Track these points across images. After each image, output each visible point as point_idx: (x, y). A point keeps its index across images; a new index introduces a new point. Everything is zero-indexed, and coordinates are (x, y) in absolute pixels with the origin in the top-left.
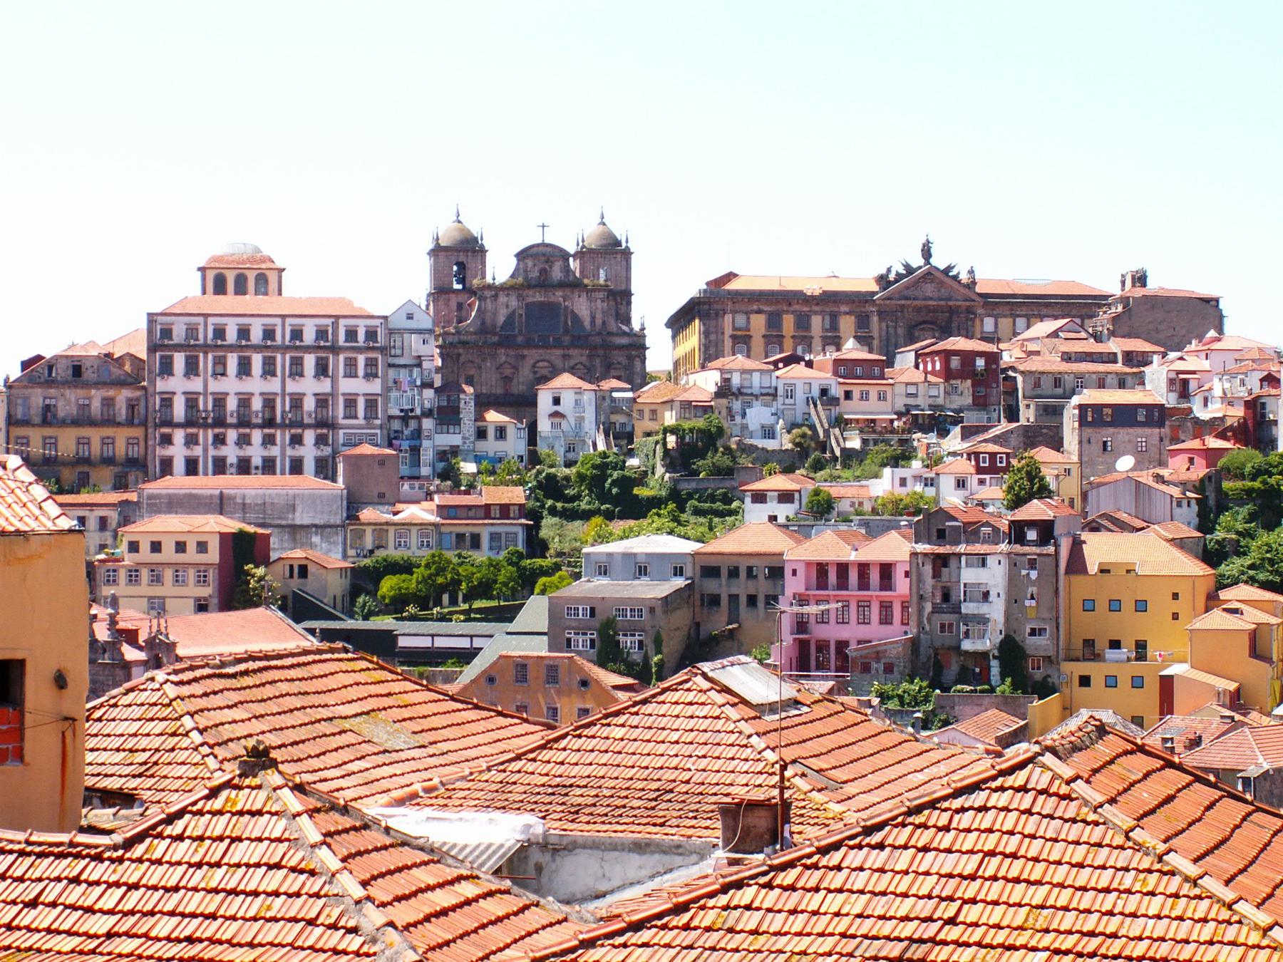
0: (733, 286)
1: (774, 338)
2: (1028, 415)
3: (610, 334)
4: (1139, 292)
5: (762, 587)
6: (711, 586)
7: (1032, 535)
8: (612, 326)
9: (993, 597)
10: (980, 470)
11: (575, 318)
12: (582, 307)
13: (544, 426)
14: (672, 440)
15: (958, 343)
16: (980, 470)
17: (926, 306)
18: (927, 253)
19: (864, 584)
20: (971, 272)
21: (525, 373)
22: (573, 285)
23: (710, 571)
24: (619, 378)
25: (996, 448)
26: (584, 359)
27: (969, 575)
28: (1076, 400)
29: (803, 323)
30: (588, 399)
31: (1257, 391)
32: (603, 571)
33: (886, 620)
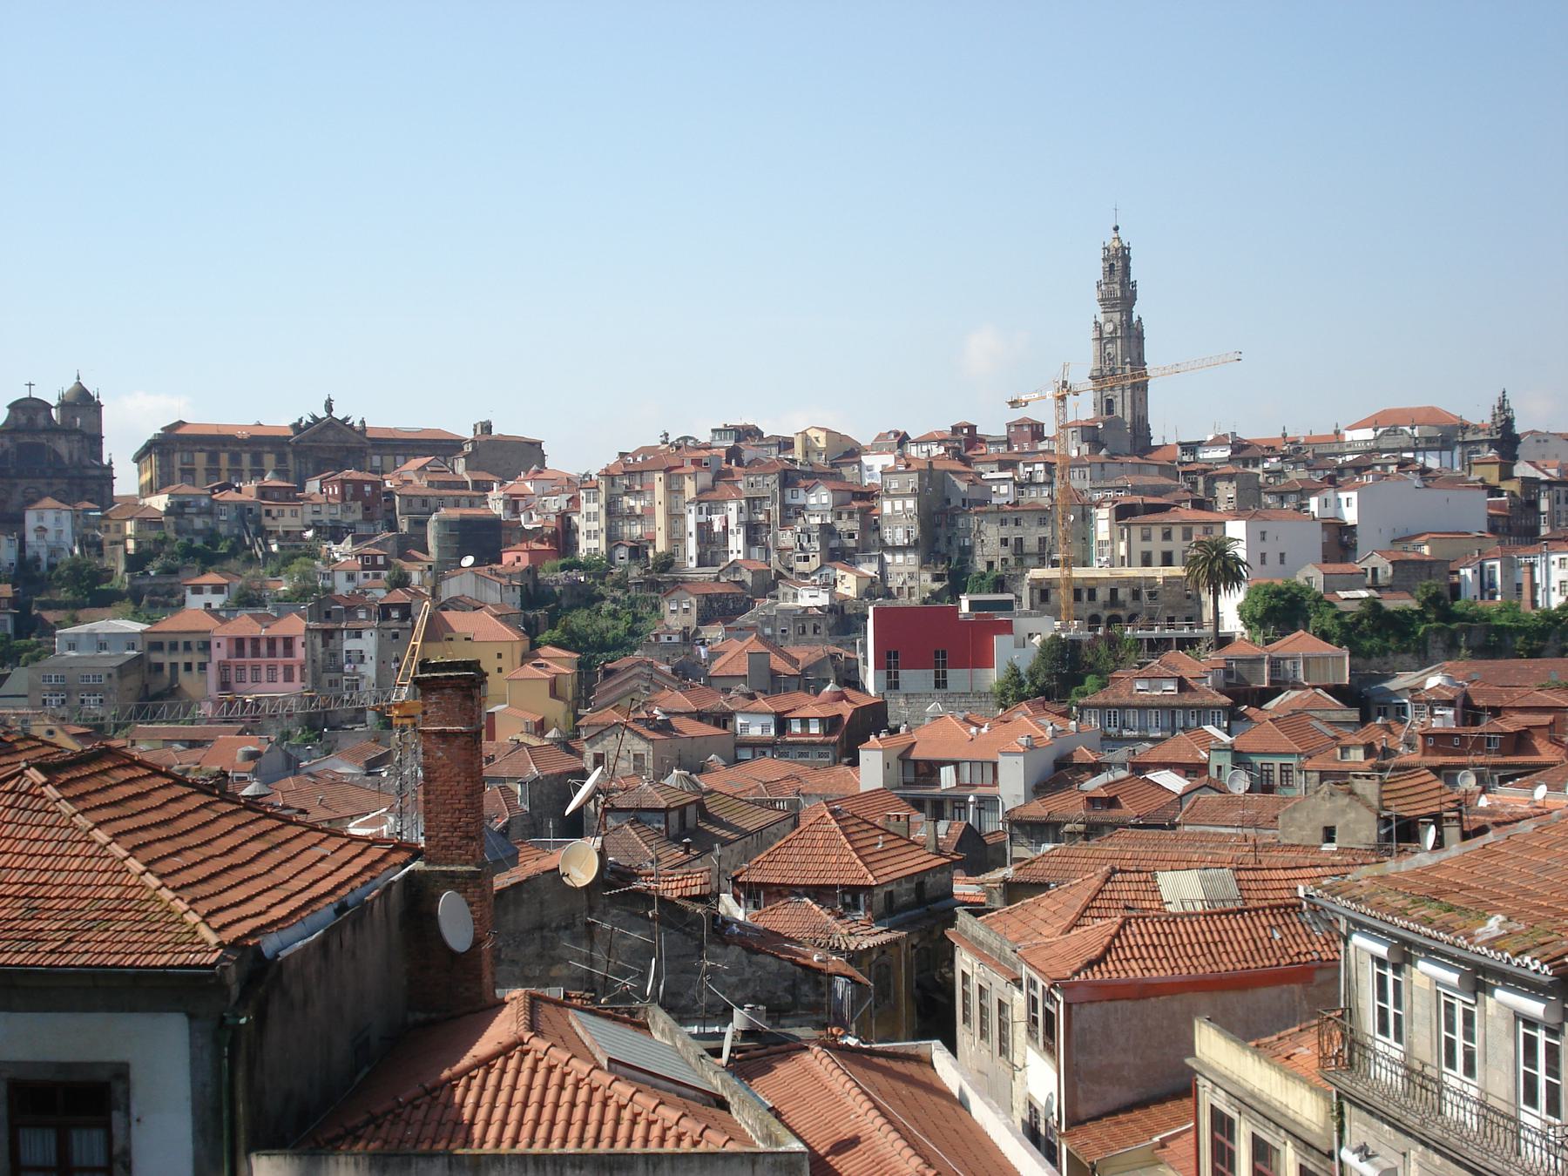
0: (183, 431)
1: (213, 472)
2: (404, 525)
3: (85, 467)
4: (485, 438)
5: (196, 658)
6: (156, 657)
7: (395, 614)
8: (87, 462)
9: (367, 659)
10: (364, 568)
11: (57, 456)
12: (62, 447)
13: (31, 537)
14: (131, 544)
15: (352, 474)
16: (364, 568)
17: (328, 445)
18: (329, 406)
19: (272, 651)
20: (363, 422)
21: (17, 498)
22: (53, 429)
23: (157, 646)
24: (91, 501)
25: (377, 551)
26: (64, 487)
27: (350, 644)
28: (434, 517)
29: (235, 459)
30: (66, 517)
31: (564, 507)
32: (72, 647)
33: (289, 678)
